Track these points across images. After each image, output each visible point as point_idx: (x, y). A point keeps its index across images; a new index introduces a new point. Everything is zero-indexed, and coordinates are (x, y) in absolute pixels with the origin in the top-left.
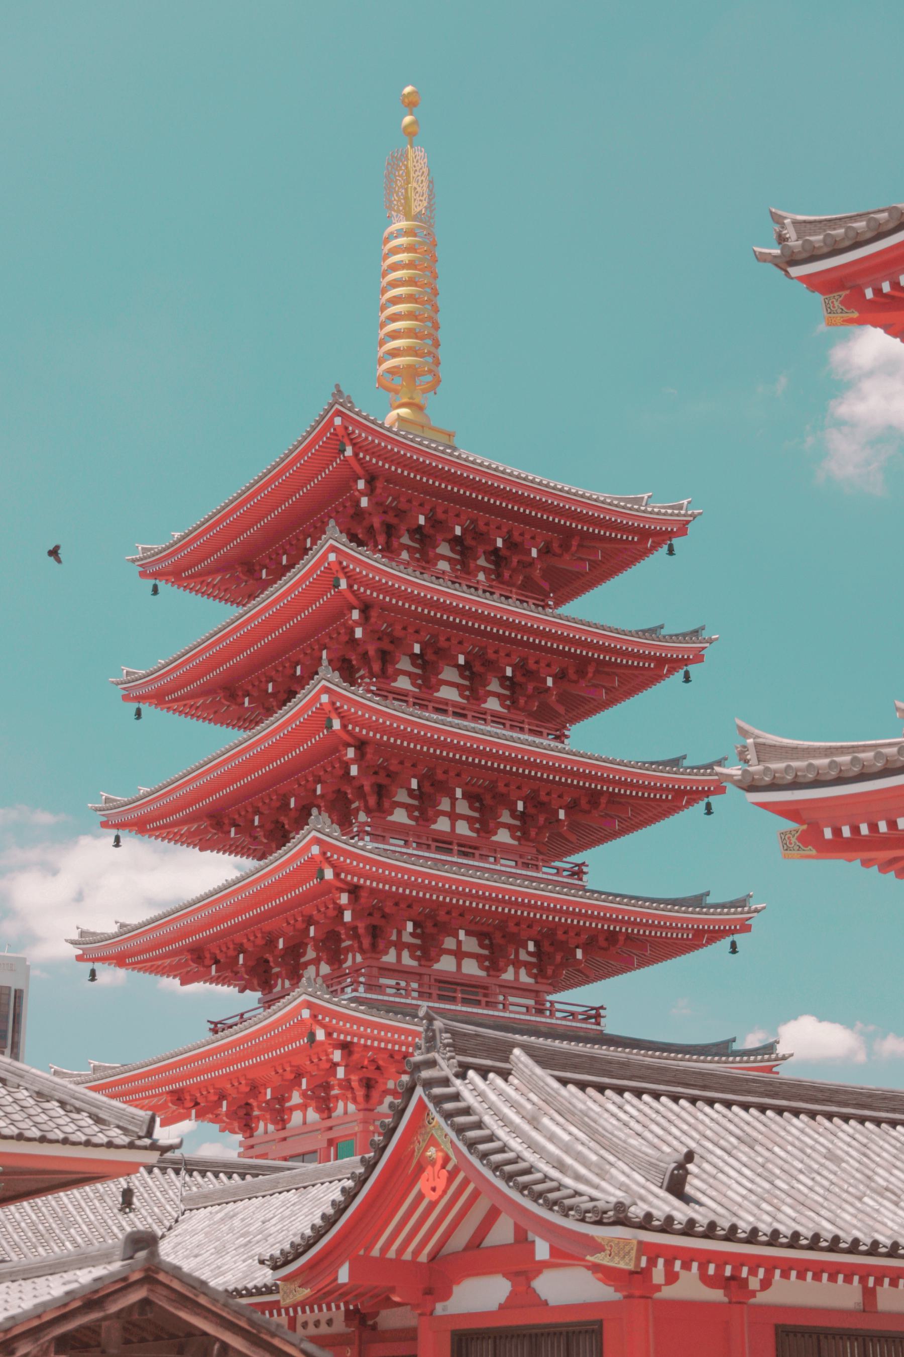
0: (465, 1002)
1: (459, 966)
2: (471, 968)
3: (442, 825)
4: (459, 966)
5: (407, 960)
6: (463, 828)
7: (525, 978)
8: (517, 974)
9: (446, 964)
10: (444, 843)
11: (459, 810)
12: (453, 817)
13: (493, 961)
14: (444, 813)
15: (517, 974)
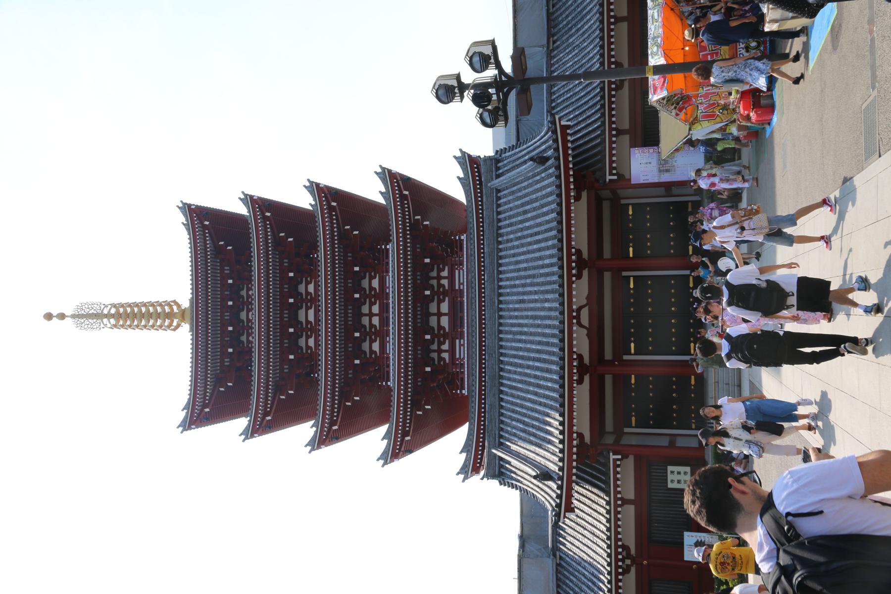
0: (462, 326)
1: (445, 314)
2: (445, 307)
3: (376, 321)
4: (445, 314)
5: (446, 347)
6: (376, 309)
7: (445, 273)
8: (445, 278)
9: (445, 322)
10: (384, 321)
11: (367, 312)
12: (371, 315)
13: (440, 294)
14: (370, 321)
15: (445, 278)
